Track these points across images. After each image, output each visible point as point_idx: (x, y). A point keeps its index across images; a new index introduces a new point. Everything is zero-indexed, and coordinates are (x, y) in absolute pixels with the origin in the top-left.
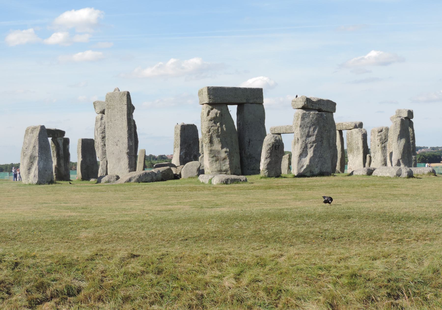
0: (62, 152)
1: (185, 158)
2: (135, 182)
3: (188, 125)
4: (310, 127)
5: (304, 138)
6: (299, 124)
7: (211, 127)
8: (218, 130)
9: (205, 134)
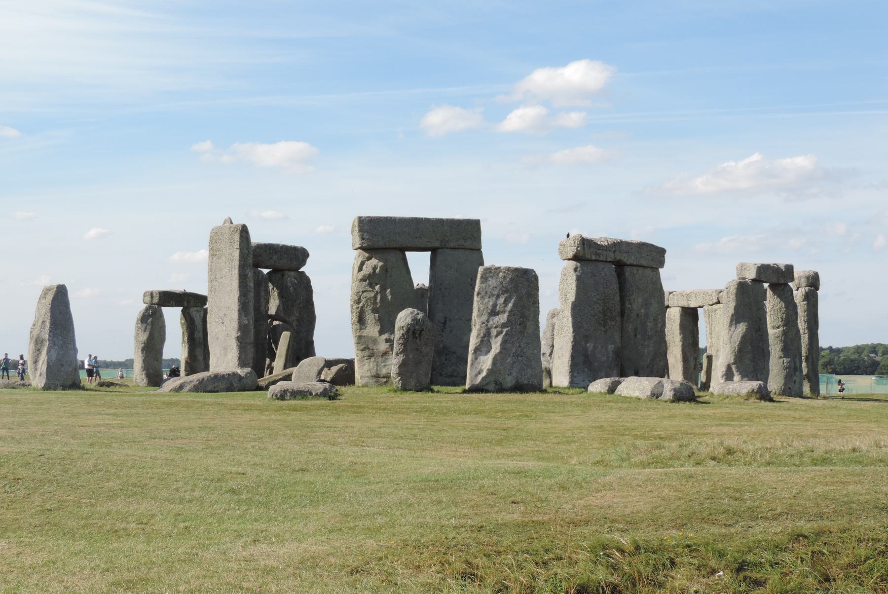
2: (190, 391)
4: (498, 297)
5: (485, 318)
7: (363, 292)
8: (375, 297)
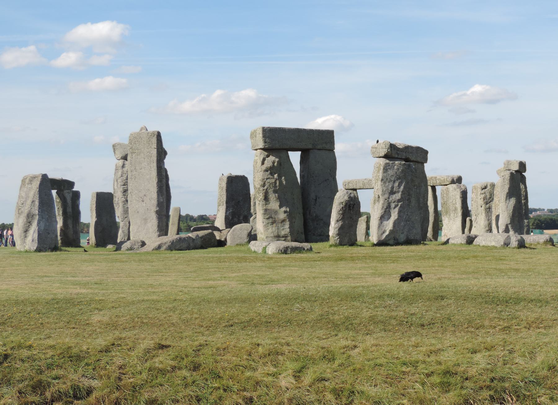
0: (69, 210)
1: (232, 219)
2: (166, 249)
3: (237, 177)
4: (394, 182)
5: (386, 196)
6: (381, 177)
7: (267, 179)
8: (275, 183)
9: (259, 188)
